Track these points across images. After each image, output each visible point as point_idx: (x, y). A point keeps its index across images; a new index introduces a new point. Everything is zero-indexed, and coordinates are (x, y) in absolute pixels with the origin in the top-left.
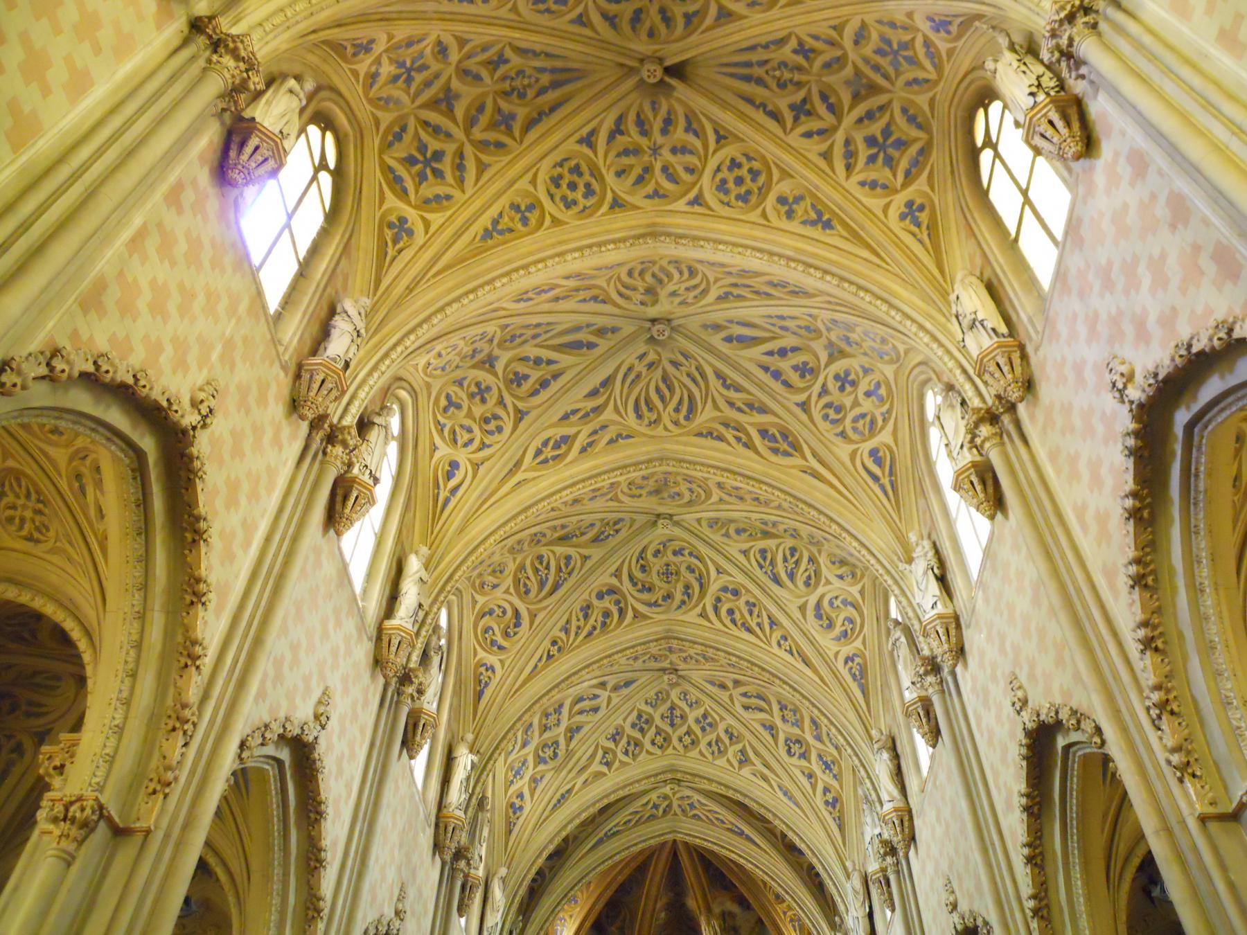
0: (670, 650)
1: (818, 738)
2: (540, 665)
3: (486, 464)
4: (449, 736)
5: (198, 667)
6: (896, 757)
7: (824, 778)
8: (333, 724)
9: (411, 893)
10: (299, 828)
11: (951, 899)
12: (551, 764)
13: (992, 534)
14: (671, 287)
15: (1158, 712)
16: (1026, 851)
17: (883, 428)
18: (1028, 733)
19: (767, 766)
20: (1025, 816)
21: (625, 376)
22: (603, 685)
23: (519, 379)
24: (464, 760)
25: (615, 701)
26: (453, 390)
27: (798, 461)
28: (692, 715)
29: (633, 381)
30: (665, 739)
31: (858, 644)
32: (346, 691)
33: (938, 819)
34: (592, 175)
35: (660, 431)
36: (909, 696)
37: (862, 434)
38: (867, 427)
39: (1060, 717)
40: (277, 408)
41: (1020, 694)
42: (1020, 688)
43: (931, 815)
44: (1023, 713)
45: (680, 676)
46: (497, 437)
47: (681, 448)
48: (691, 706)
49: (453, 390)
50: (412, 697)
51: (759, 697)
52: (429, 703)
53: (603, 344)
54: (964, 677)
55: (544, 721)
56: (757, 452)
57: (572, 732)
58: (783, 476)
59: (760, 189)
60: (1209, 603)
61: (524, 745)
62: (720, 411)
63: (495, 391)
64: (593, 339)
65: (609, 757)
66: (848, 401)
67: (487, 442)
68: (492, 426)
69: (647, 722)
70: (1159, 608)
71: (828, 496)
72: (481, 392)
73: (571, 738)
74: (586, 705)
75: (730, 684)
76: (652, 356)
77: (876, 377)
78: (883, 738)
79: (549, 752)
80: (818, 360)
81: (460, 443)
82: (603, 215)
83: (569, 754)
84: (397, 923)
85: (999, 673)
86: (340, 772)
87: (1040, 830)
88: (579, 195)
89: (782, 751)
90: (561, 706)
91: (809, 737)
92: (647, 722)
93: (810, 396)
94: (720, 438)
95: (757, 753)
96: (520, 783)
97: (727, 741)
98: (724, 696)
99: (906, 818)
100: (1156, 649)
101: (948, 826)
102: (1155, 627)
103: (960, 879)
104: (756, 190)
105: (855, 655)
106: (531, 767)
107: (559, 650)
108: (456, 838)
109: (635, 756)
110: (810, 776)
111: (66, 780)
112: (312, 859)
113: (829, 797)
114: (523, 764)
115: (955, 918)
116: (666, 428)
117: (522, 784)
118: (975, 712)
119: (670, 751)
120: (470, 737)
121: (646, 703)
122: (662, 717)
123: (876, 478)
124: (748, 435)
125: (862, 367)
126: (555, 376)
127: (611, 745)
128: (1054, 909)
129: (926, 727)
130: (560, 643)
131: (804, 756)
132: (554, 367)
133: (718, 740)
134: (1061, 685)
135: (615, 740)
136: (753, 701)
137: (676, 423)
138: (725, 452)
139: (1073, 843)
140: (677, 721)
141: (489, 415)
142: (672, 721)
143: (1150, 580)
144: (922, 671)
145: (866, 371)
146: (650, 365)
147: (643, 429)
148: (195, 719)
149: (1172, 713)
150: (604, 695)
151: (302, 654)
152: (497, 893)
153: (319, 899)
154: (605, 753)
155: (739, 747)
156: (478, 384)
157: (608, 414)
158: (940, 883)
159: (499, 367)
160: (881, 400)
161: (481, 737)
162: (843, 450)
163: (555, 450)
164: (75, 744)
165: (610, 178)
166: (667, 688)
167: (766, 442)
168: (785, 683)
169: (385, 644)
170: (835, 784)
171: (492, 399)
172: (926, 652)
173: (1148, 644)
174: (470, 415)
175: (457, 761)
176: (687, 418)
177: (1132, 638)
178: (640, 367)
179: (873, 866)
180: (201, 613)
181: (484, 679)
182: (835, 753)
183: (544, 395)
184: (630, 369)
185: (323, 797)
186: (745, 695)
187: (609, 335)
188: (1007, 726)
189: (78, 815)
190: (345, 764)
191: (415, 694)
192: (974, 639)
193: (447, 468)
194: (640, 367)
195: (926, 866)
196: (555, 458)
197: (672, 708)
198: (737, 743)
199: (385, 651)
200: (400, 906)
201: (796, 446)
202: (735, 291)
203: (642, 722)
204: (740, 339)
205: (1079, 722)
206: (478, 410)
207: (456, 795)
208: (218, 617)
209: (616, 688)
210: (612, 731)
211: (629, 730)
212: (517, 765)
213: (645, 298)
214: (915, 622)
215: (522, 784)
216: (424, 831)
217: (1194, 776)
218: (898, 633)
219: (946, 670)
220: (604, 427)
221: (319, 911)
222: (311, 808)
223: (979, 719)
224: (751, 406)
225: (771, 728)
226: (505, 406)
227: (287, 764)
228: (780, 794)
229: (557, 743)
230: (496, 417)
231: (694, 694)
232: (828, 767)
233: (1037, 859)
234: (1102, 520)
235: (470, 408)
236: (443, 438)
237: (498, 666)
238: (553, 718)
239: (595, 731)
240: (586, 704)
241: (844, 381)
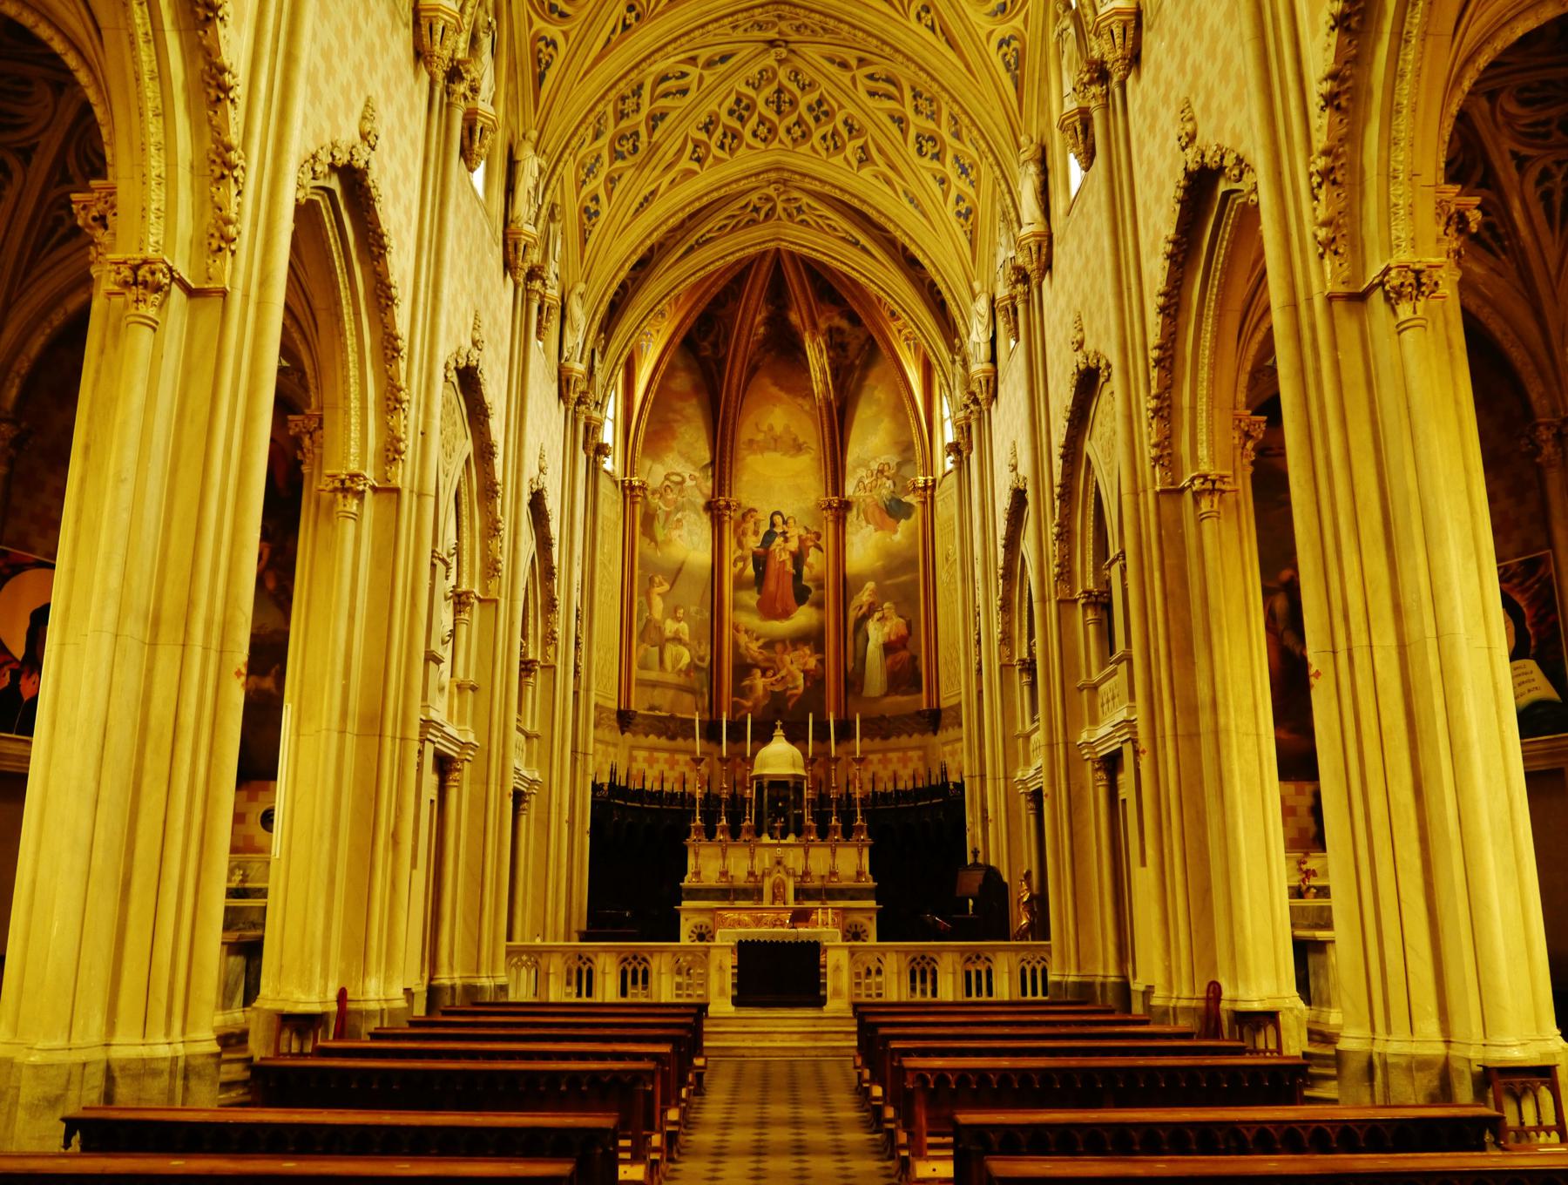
0: (780, 17)
1: (957, 135)
2: (614, 38)
4: (508, 133)
5: (232, 101)
6: (1044, 172)
7: (958, 184)
8: (382, 143)
9: (486, 321)
10: (362, 263)
11: (1079, 337)
12: (631, 160)
16: (1161, 300)
18: (1189, 175)
19: (893, 167)
20: (1167, 264)
22: (693, 60)
24: (530, 166)
25: (708, 80)
28: (804, 101)
30: (769, 131)
31: (1018, 22)
32: (389, 98)
33: (1079, 248)
36: (1071, 105)
39: (1225, 163)
41: (1189, 127)
42: (1191, 119)
43: (1072, 244)
44: (1188, 151)
45: (793, 51)
48: (803, 89)
50: (466, 98)
51: (888, 80)
52: (483, 105)
54: (1134, 91)
55: (620, 106)
57: (656, 119)
60: (1410, 57)
61: (597, 136)
65: (701, 151)
69: (747, 108)
70: (1356, 57)
73: (654, 128)
74: (672, 85)
75: (854, 63)
78: (1033, 147)
79: (628, 145)
83: (654, 148)
84: (475, 353)
85: (1173, 95)
86: (397, 196)
87: (1181, 279)
89: (912, 149)
90: (640, 86)
91: (945, 133)
92: (747, 108)
95: (880, 150)
96: (595, 183)
97: (845, 135)
98: (845, 78)
99: (1045, 246)
100: (1338, 108)
101: (1088, 259)
102: (1344, 80)
103: (1091, 315)
105: (1012, 37)
106: (606, 163)
107: (638, 17)
108: (528, 257)
109: (732, 151)
110: (942, 181)
111: (114, 234)
113: (963, 207)
114: (597, 159)
115: (1079, 356)
117: (597, 184)
118: (1139, 137)
119: (775, 144)
120: (534, 134)
121: (747, 83)
122: (767, 102)
127: (703, 136)
128: (1178, 364)
129: (1081, 147)
130: (638, 8)
131: (936, 157)
133: (835, 133)
134: (1235, 127)
135: (707, 131)
136: (882, 85)
139: (1212, 293)
140: (786, 108)
142: (779, 107)
143: (1354, 23)
144: (1086, 78)
148: (241, 163)
149: (1334, 182)
150: (694, 72)
151: (335, 60)
152: (578, 312)
153: (396, 338)
154: (696, 146)
155: (860, 142)
158: (1070, 319)
161: (547, 134)
164: (112, 192)
166: (775, 65)
168: (922, 69)
169: (425, 30)
170: (971, 191)
172: (1096, 54)
173: (1330, 100)
175: (520, 167)
177: (1317, 88)
179: (1002, 292)
180: (221, 32)
181: (544, 58)
182: (975, 155)
185: (384, 228)
186: (871, 77)
188: (1169, 160)
189: (149, 278)
190: (401, 187)
191: (468, 93)
192: (1155, 47)
195: (1058, 297)
197: (779, 91)
198: (857, 137)
199: (426, 40)
200: (477, 337)
203: (742, 108)
205: (1241, 173)
207: (523, 208)
208: (239, 30)
209: (710, 64)
210: (704, 118)
211: (724, 118)
212: (589, 162)
214: (1089, 11)
215: (597, 184)
216: (492, 251)
217: (1336, 253)
218: (1067, 22)
219: (1115, 79)
221: (398, 350)
222: (373, 243)
223: (1141, 145)
225: (900, 121)
228: (905, 201)
229: (636, 134)
231: (808, 74)
232: (964, 171)
233: (1173, 306)
237: (560, 40)
238: (631, 102)
239: (683, 124)
240: (671, 84)
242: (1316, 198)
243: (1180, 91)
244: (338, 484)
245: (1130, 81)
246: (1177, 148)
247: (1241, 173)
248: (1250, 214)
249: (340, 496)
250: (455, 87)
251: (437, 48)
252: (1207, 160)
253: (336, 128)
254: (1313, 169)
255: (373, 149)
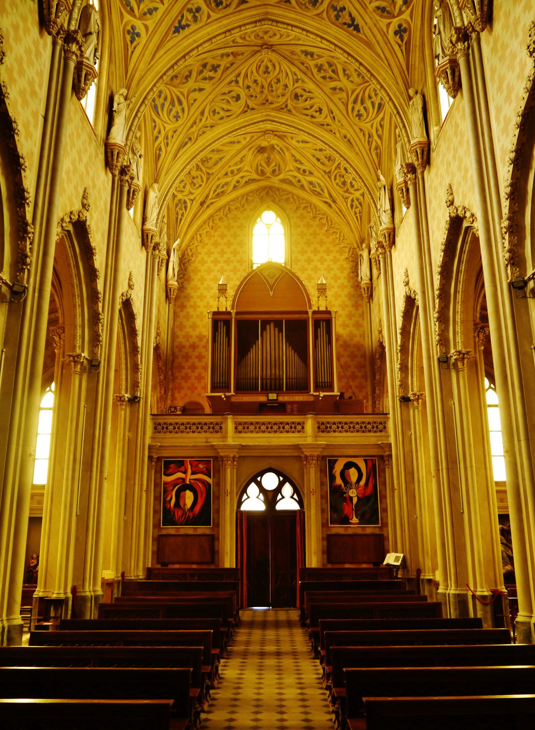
11: (406, 280)
13: (454, 103)
15: (505, 230)
40: (35, 30)
44: (450, 208)
112: (92, 273)
134: (470, 200)
222: (88, 252)
227: (72, 232)
234: (507, 121)
242: (504, 238)
243: (447, 182)
244: (71, 358)
245: (426, 173)
246: (446, 207)
247: (473, 221)
248: (476, 240)
249: (73, 364)
250: (123, 177)
251: (115, 162)
252: (459, 212)
253: (72, 204)
254: (503, 225)
255: (88, 211)
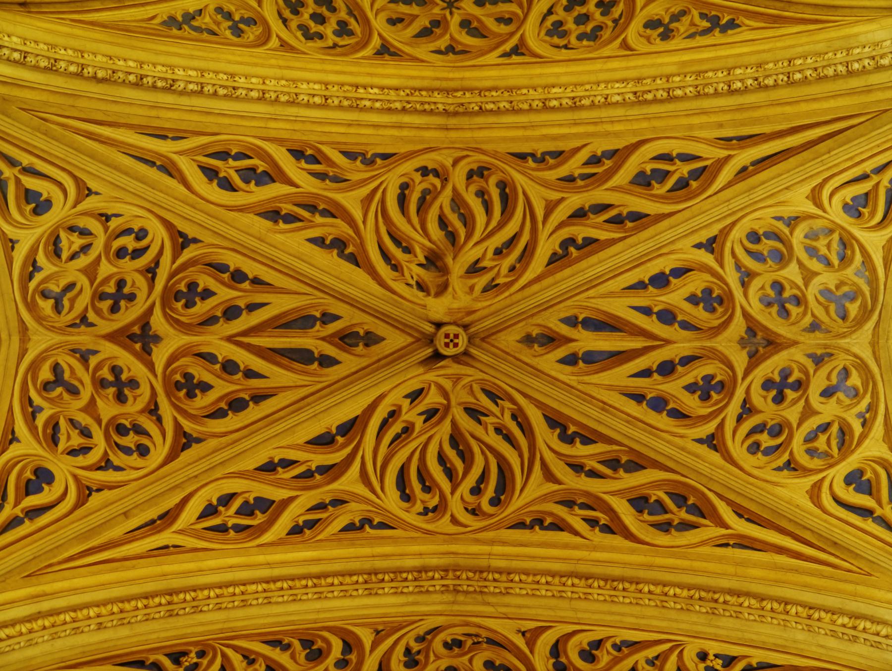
3: (106, 494)
14: (470, 254)
17: (863, 437)
21: (384, 425)
23: (192, 387)
26: (67, 361)
27: (713, 531)
29: (397, 437)
34: (350, 13)
35: (444, 524)
37: (827, 455)
38: (834, 443)
46: (134, 460)
47: (486, 549)
49: (67, 361)
53: (349, 362)
56: (629, 535)
58: (685, 563)
59: (616, 21)
62: (557, 481)
63: (145, 391)
64: (331, 351)
66: (792, 414)
67: (116, 461)
68: (130, 440)
71: (776, 567)
72: (121, 386)
76: (433, 398)
77: (841, 361)
80: (731, 367)
81: (62, 446)
82: (363, 58)
88: (329, 30)
93: (721, 426)
94: (559, 526)
104: (610, 23)
116: (454, 521)
123: (865, 512)
124: (610, 511)
125: (809, 356)
126: (259, 398)
132: (255, 383)
137: (474, 512)
138: (566, 546)
141: (127, 423)
145: (818, 361)
146: (430, 414)
147: (411, 518)
156: (116, 370)
157: (349, 482)
159: (160, 355)
160: (856, 394)
162: (792, 492)
163: (241, 518)
165: (379, 24)
167: (646, 516)
171: (134, 406)
174: (90, 408)
176: (495, 502)
178: (412, 415)
183: (233, 421)
184: (393, 414)
187: (360, 349)
193: (28, 474)
194: (412, 415)
196: (239, 529)
201: (703, 511)
202: (581, 232)
204: (591, 358)
206: (108, 409)
213: (426, 276)
220: (338, 502)
224: (614, 464)
226: (159, 420)
230: (139, 430)
235: (92, 401)
236: (33, 429)
241: (778, 388)
